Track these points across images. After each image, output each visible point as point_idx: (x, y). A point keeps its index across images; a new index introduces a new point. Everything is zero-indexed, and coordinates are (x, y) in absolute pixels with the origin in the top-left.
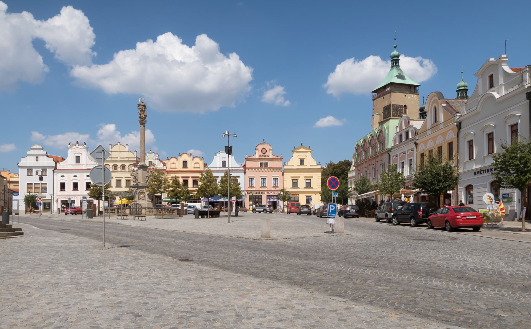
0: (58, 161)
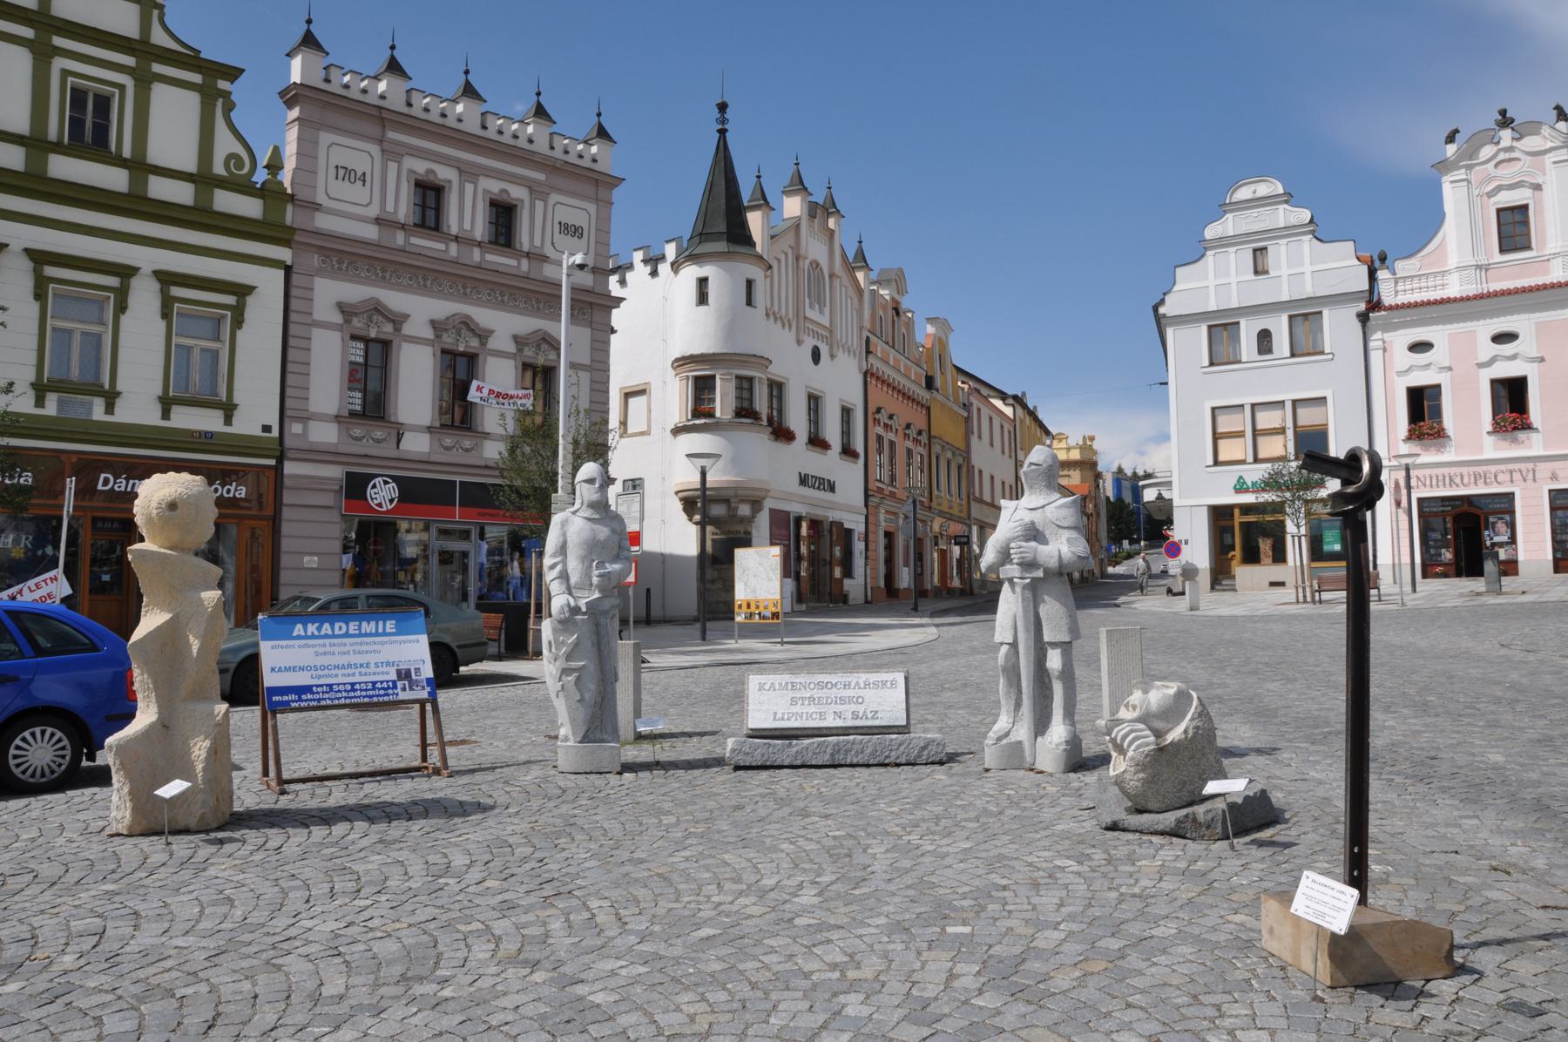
0: (1383, 259)
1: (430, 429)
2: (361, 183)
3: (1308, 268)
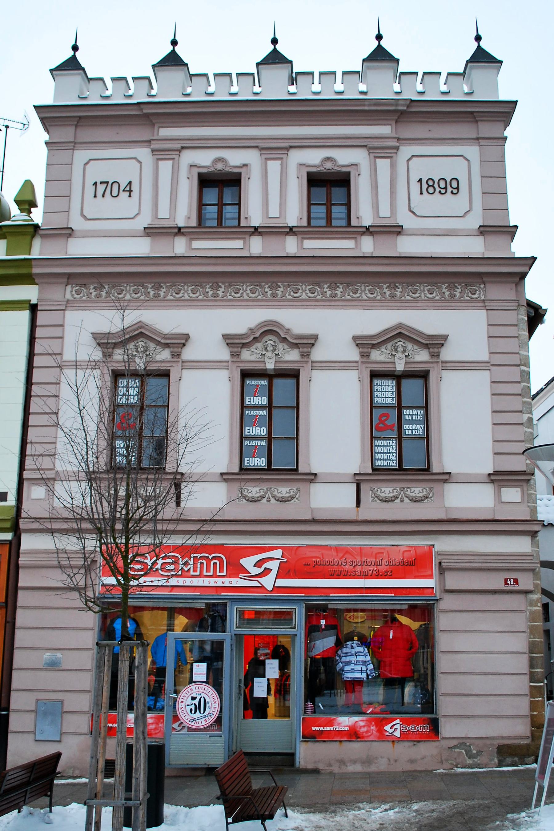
1: (225, 477)
2: (128, 193)
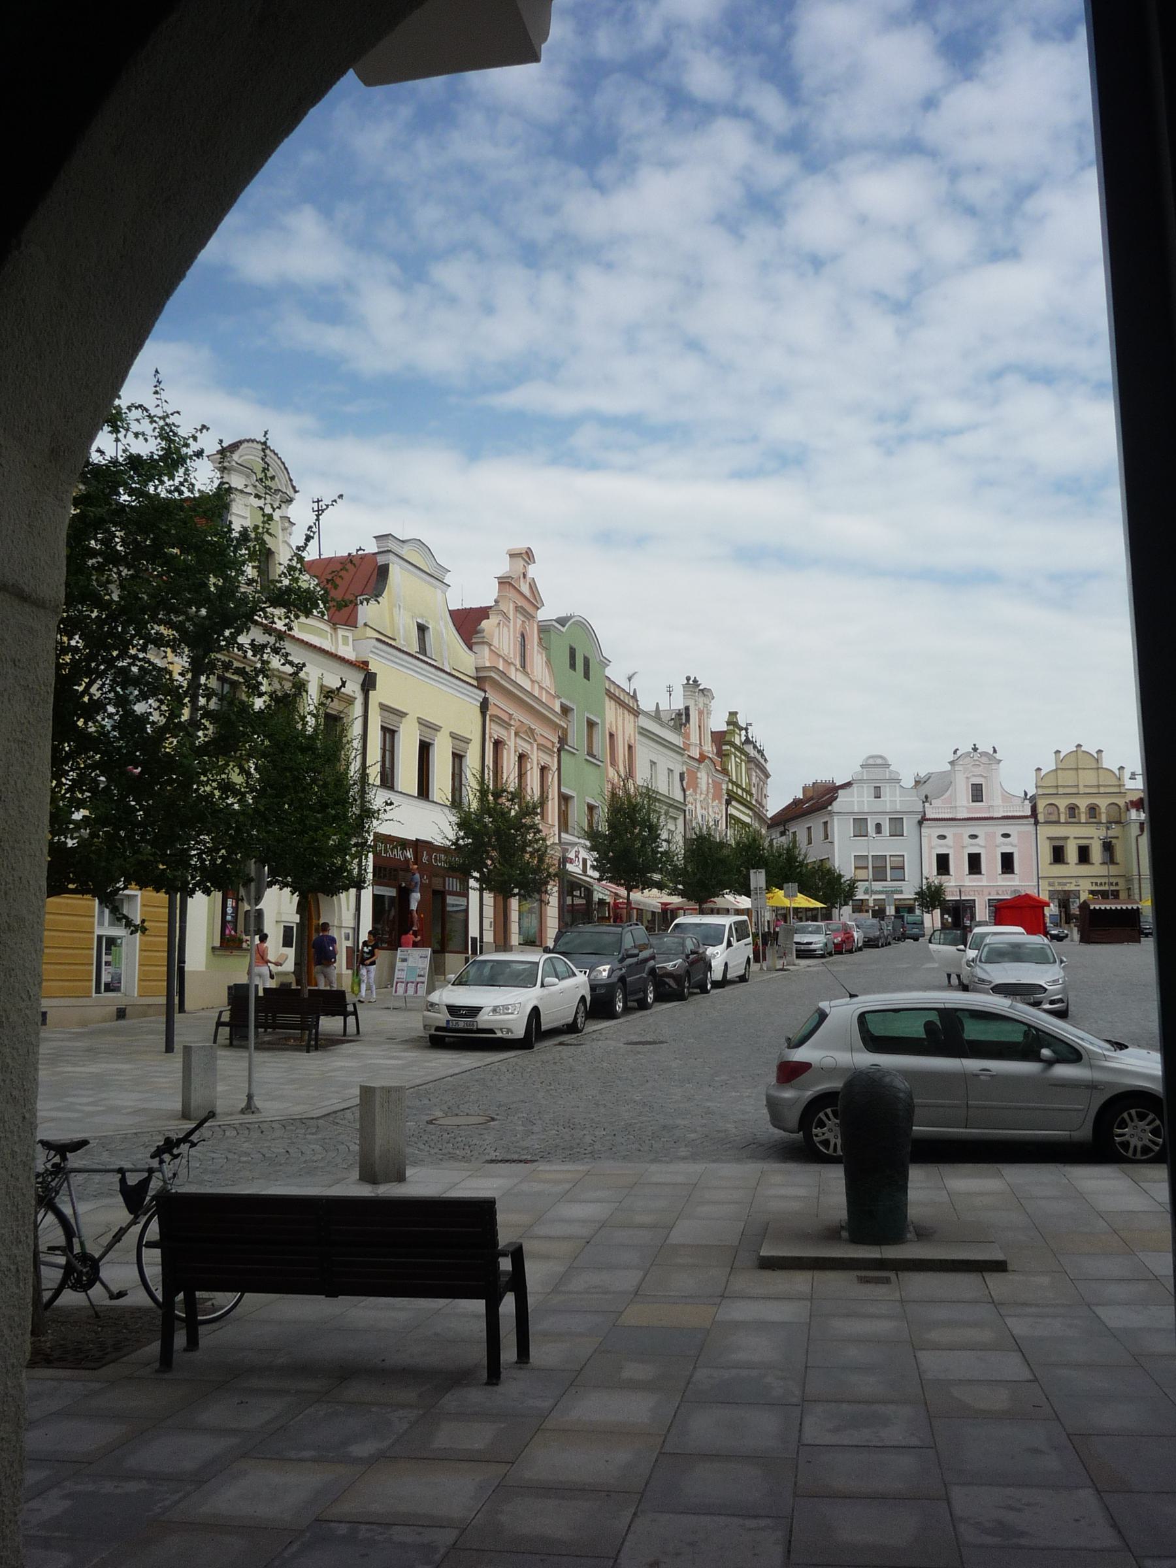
0: (926, 797)
3: (898, 799)
